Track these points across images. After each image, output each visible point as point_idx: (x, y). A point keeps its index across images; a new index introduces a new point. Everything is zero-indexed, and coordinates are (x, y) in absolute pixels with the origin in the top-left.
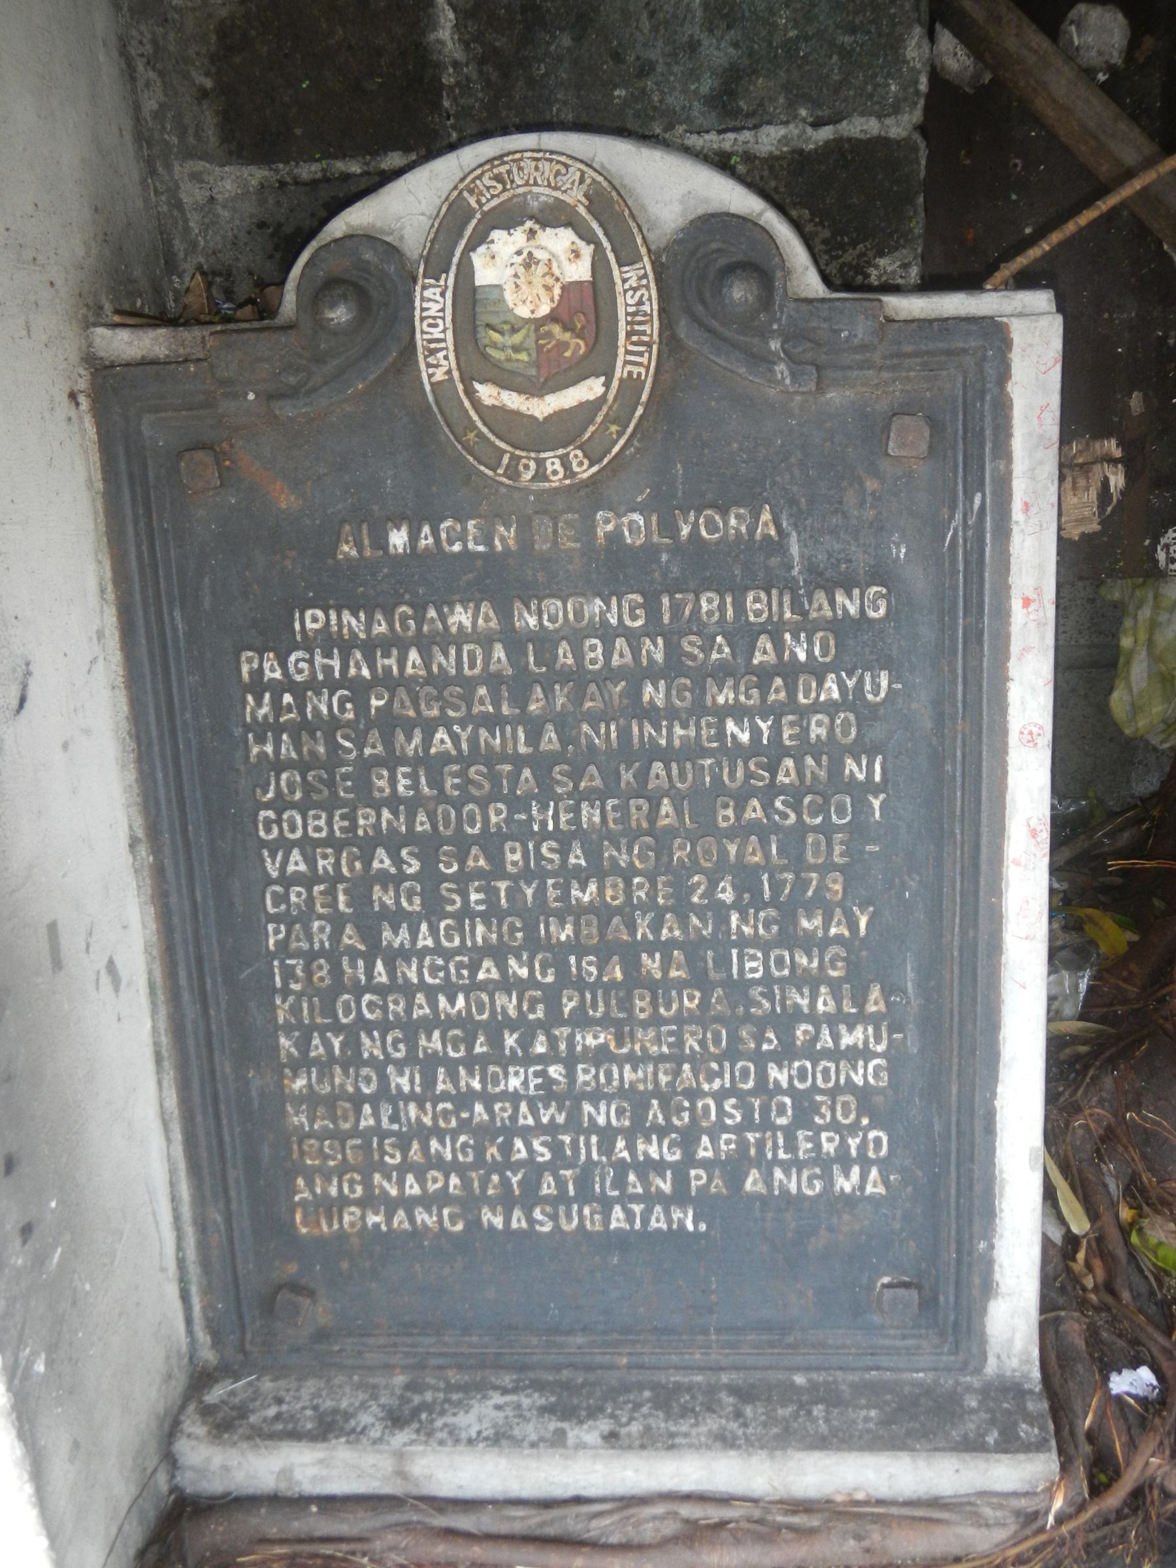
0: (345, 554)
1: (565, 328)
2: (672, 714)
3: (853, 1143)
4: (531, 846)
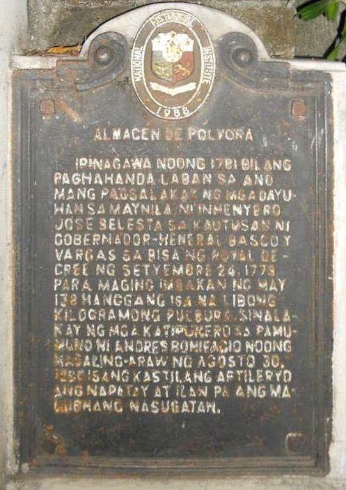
0: (97, 139)
1: (183, 66)
2: (214, 202)
3: (278, 375)
4: (158, 251)
